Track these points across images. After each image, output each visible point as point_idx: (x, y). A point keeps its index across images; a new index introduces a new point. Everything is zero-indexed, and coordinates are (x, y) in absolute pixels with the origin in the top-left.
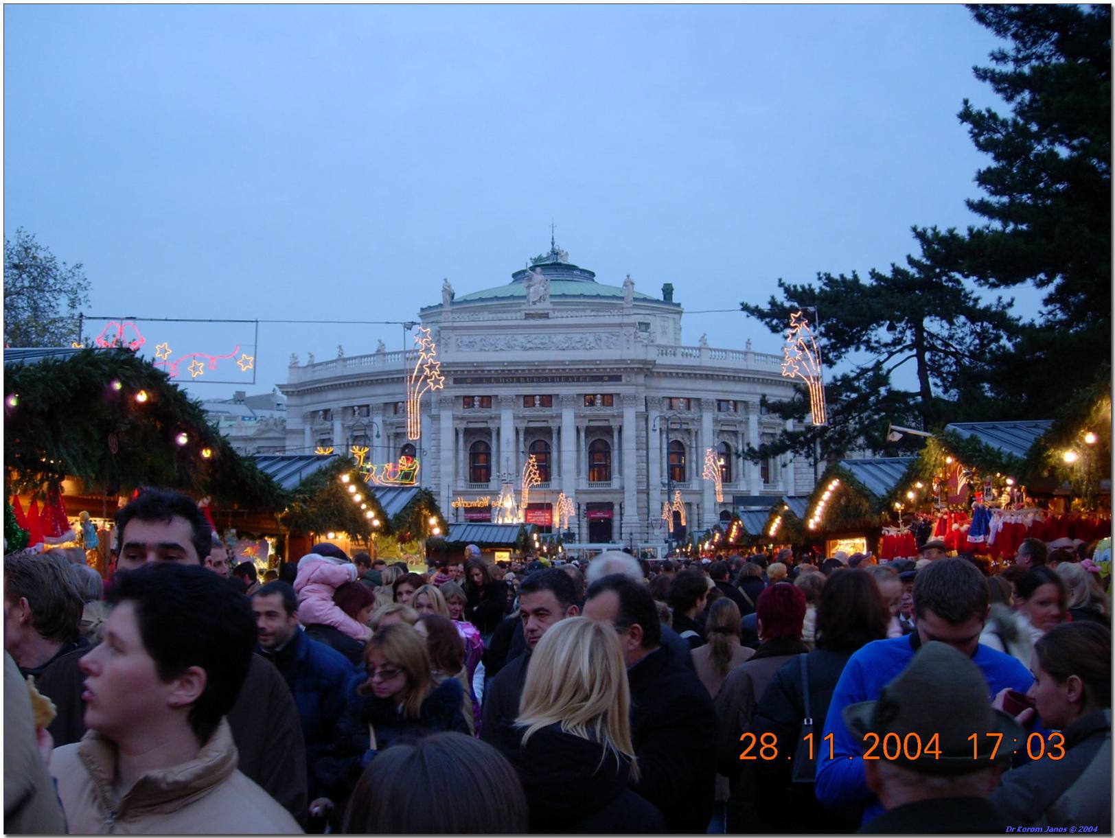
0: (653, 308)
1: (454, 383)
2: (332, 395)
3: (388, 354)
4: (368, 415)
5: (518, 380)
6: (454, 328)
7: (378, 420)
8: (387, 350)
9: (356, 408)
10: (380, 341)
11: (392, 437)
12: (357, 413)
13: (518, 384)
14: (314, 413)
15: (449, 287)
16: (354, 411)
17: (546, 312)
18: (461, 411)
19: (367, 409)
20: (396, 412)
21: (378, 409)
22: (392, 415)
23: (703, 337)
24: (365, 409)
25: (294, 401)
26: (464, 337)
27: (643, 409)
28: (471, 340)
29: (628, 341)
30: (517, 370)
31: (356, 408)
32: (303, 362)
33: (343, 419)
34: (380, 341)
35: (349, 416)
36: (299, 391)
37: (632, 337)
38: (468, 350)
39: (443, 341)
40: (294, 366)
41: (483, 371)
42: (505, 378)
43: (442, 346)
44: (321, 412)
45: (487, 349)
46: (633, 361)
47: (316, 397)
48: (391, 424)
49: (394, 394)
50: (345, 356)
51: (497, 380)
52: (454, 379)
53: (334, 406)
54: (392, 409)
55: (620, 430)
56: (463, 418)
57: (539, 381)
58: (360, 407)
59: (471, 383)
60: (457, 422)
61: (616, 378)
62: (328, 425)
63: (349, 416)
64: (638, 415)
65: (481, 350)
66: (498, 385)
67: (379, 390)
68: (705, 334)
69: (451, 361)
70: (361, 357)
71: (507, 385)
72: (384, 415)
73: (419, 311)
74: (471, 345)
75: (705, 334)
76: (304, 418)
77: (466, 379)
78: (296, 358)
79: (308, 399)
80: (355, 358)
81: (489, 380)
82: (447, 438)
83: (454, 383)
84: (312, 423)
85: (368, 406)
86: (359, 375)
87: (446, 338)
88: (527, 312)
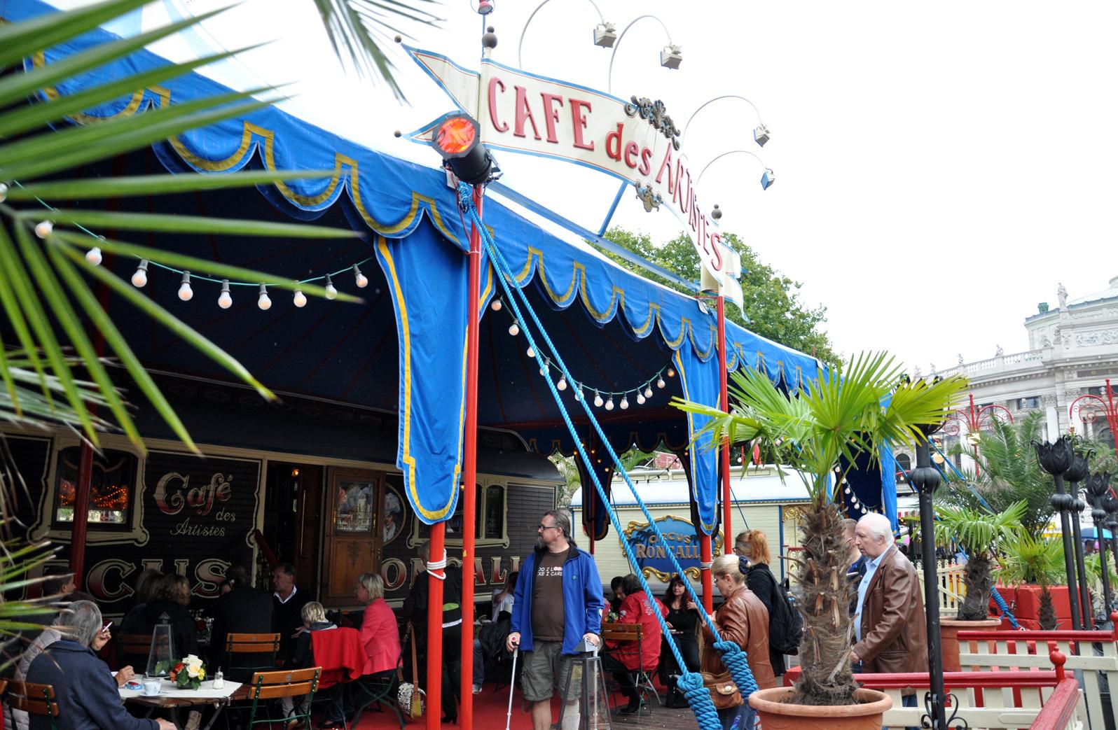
1: (1079, 376)
6: (1073, 327)
8: (1005, 354)
9: (980, 407)
15: (1064, 290)
20: (1019, 408)
26: (1084, 335)
28: (1092, 336)
31: (980, 407)
34: (998, 346)
38: (1090, 344)
39: (1063, 339)
43: (1063, 343)
45: (1109, 342)
50: (965, 363)
52: (1078, 372)
54: (1015, 405)
58: (983, 405)
65: (1104, 344)
69: (1073, 356)
70: (981, 362)
74: (1092, 340)
77: (1090, 371)
80: (975, 363)
83: (1079, 376)
86: (981, 378)
87: (1066, 336)
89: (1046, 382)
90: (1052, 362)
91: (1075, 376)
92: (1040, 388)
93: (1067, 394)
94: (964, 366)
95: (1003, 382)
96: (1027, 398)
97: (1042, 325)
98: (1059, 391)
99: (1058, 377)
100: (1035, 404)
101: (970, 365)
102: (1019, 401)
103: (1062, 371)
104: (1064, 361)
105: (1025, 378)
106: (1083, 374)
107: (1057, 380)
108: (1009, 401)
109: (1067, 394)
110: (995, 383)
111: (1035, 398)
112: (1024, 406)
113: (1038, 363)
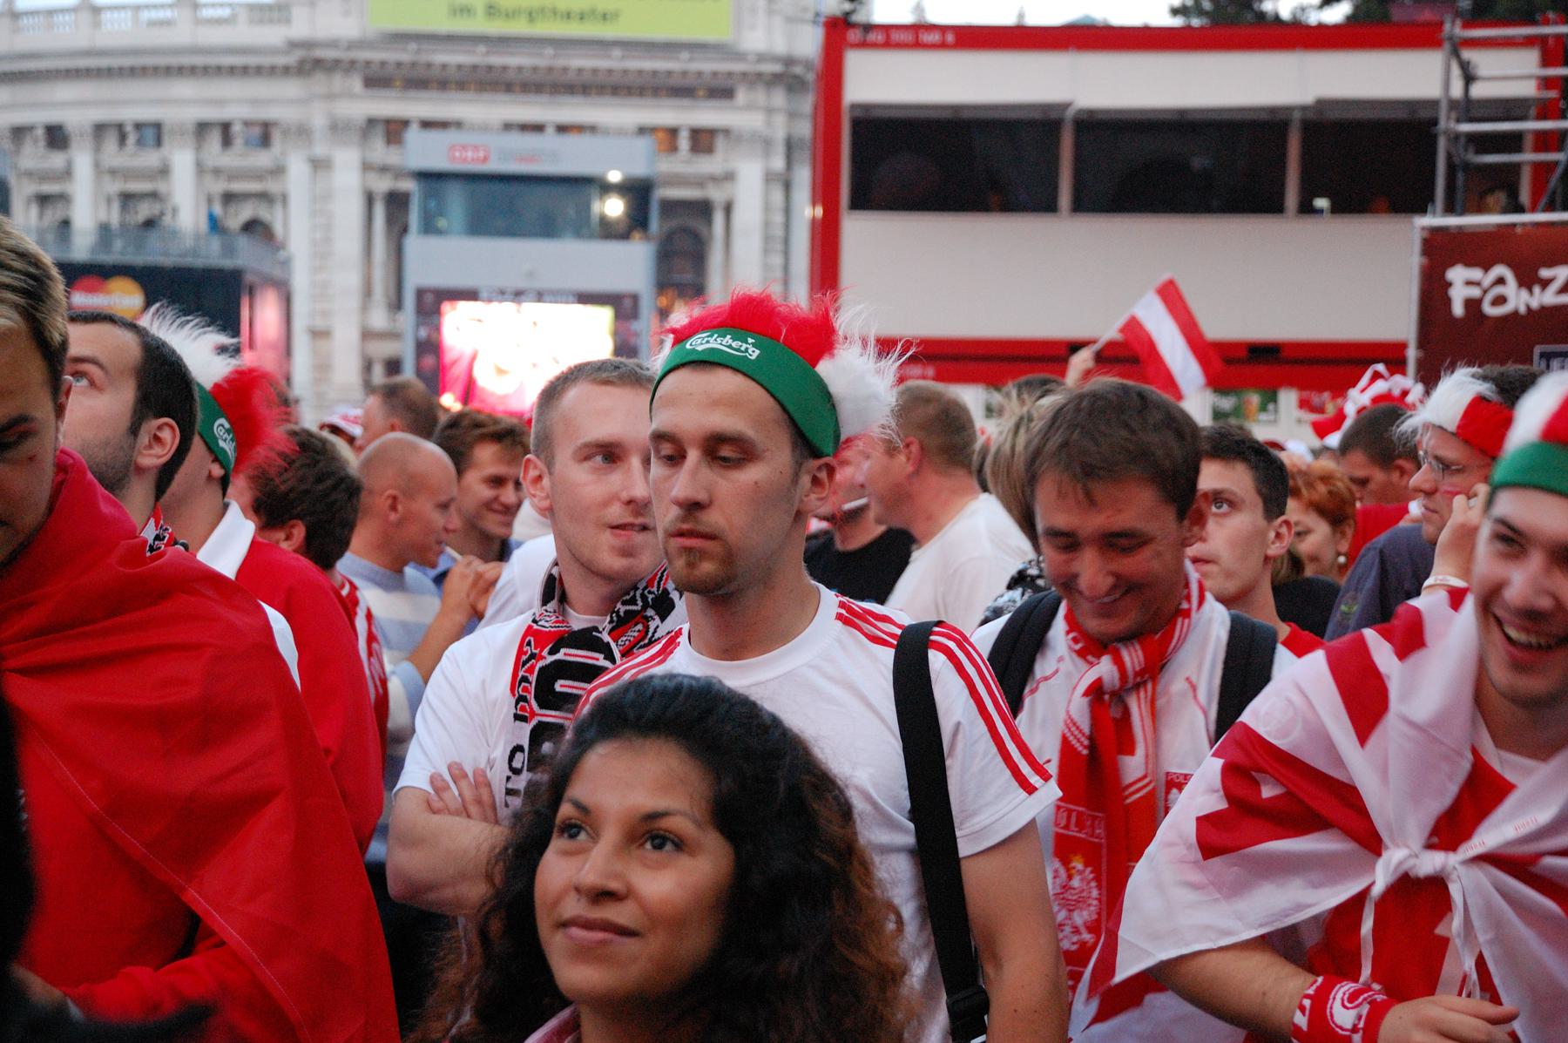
4: (159, 142)
5: (509, 87)
7: (182, 160)
16: (122, 138)
18: (380, 151)
19: (152, 133)
20: (227, 141)
27: (778, 163)
31: (129, 128)
33: (98, 149)
35: (111, 144)
44: (40, 132)
46: (762, 58)
47: (24, 92)
51: (462, 86)
53: (76, 119)
54: (215, 139)
55: (728, 209)
56: (384, 169)
58: (139, 126)
61: (721, 91)
62: (57, 160)
63: (111, 144)
64: (769, 178)
67: (184, 89)
72: (198, 148)
80: (123, 8)
82: (349, 211)
89: (291, 88)
91: (356, 83)
93: (337, 128)
95: (192, 71)
98: (318, 118)
99: (319, 83)
100: (265, 140)
102: (226, 127)
104: (333, 44)
105: (244, 71)
106: (377, 80)
108: (202, 128)
109: (337, 128)
110: (170, 72)
112: (238, 142)
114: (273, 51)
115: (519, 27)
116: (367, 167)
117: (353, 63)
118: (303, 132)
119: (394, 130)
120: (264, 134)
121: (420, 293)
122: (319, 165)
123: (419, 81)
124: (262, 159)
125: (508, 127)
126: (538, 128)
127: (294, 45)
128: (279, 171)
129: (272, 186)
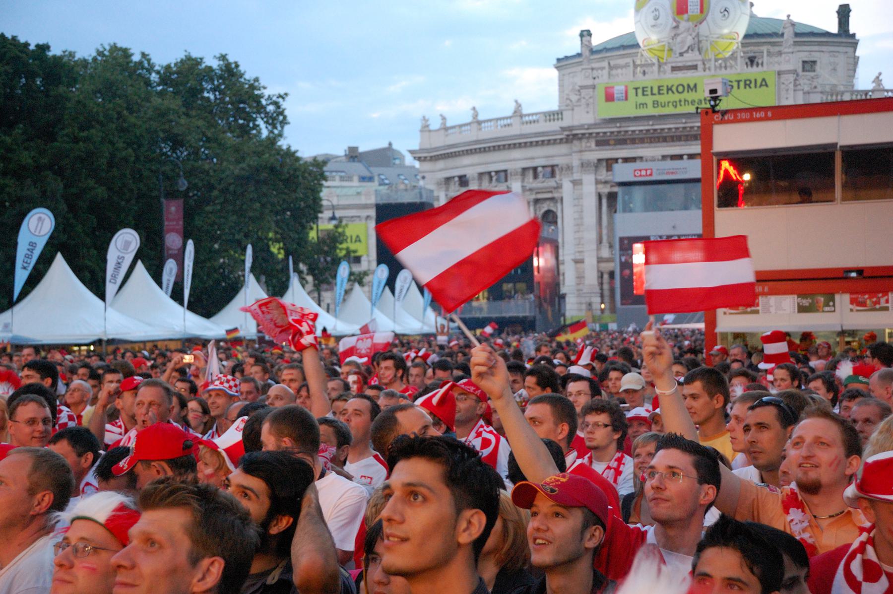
0: (820, 44)
2: (467, 160)
3: (526, 115)
4: (506, 180)
10: (516, 102)
11: (532, 204)
12: (494, 179)
13: (665, 144)
14: (448, 180)
16: (491, 178)
17: (695, 63)
18: (603, 175)
20: (536, 176)
21: (516, 174)
22: (531, 180)
23: (878, 78)
24: (502, 174)
25: (427, 166)
29: (787, 90)
30: (662, 130)
31: (493, 174)
32: (435, 125)
34: (516, 102)
36: (431, 157)
37: (791, 86)
40: (425, 128)
41: (626, 132)
42: (651, 138)
44: (456, 179)
47: (451, 162)
48: (531, 190)
49: (533, 158)
51: (642, 141)
54: (530, 174)
56: (606, 182)
57: (687, 140)
58: (497, 172)
59: (615, 144)
60: (600, 186)
66: (643, 145)
67: (516, 154)
68: (880, 74)
71: (653, 145)
72: (523, 181)
73: (555, 62)
75: (880, 74)
76: (439, 184)
77: (609, 140)
78: (427, 121)
79: (441, 164)
80: (490, 120)
81: (633, 141)
82: (591, 203)
84: (447, 190)
85: (505, 171)
87: (587, 98)
88: (674, 65)
89: (563, 149)
90: (570, 128)
91: (593, 144)
92: (558, 155)
93: (584, 165)
94: (479, 123)
96: (543, 167)
97: (573, 70)
100: (553, 174)
101: (485, 121)
102: (535, 169)
103: (580, 139)
104: (581, 127)
106: (602, 143)
107: (575, 149)
108: (524, 170)
109: (584, 165)
110: (510, 147)
111: (553, 167)
112: (541, 175)
113: (555, 126)
114: (554, 133)
115: (669, 110)
116: (598, 182)
117: (591, 134)
118: (569, 168)
119: (610, 163)
120: (552, 170)
121: (622, 240)
122: (576, 183)
123: (622, 141)
124: (551, 183)
125: (664, 157)
126: (680, 157)
127: (563, 129)
128: (559, 187)
129: (556, 195)
